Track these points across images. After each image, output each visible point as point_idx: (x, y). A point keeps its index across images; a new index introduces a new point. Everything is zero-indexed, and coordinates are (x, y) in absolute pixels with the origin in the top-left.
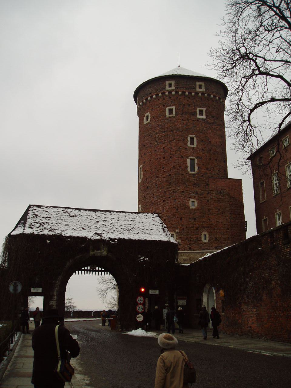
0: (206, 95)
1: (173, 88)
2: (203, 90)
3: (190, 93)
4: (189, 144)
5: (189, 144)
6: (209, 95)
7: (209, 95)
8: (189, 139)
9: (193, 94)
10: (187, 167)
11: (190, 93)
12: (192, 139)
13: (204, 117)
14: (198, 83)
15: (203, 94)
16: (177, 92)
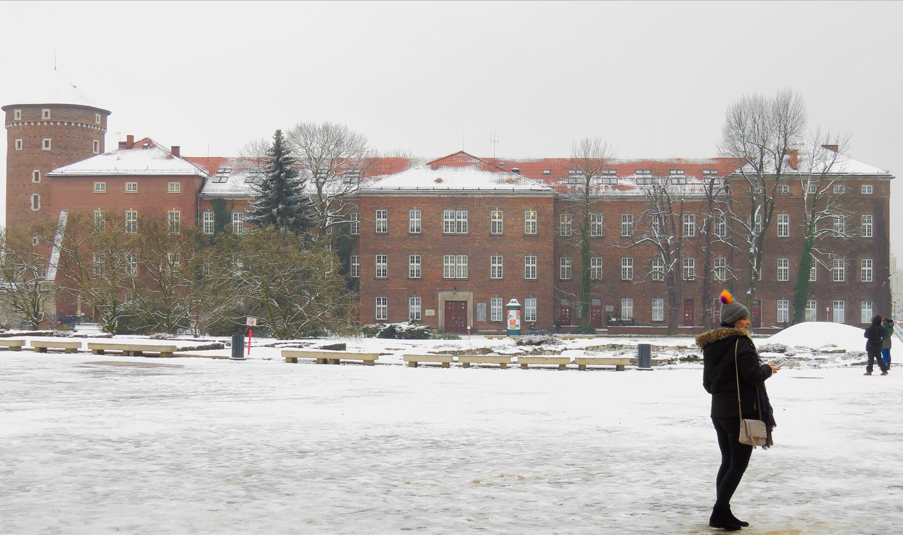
0: (52, 124)
1: (20, 118)
2: (49, 117)
3: (35, 123)
4: (33, 180)
5: (33, 180)
6: (55, 123)
7: (55, 123)
8: (34, 174)
9: (39, 124)
10: (30, 205)
11: (35, 123)
12: (37, 174)
13: (49, 149)
14: (44, 111)
15: (48, 122)
16: (23, 123)
